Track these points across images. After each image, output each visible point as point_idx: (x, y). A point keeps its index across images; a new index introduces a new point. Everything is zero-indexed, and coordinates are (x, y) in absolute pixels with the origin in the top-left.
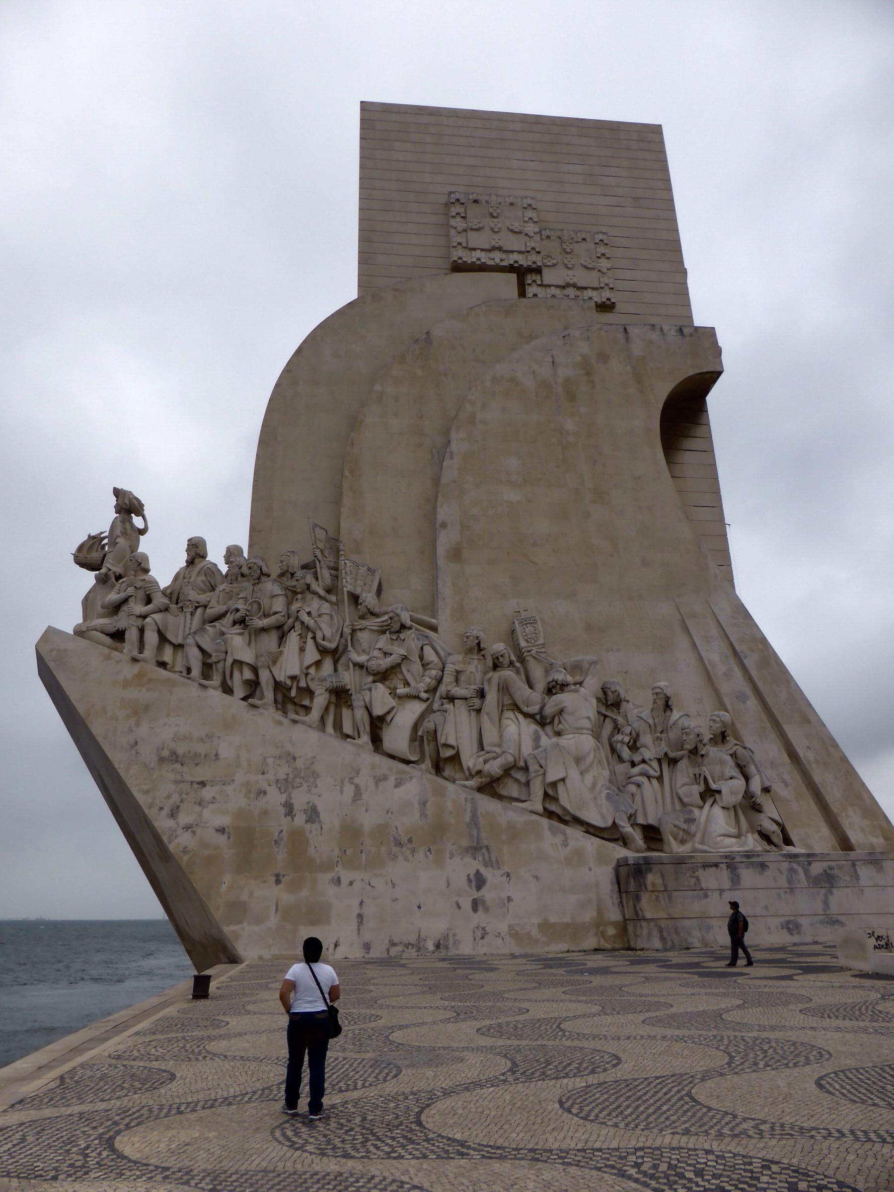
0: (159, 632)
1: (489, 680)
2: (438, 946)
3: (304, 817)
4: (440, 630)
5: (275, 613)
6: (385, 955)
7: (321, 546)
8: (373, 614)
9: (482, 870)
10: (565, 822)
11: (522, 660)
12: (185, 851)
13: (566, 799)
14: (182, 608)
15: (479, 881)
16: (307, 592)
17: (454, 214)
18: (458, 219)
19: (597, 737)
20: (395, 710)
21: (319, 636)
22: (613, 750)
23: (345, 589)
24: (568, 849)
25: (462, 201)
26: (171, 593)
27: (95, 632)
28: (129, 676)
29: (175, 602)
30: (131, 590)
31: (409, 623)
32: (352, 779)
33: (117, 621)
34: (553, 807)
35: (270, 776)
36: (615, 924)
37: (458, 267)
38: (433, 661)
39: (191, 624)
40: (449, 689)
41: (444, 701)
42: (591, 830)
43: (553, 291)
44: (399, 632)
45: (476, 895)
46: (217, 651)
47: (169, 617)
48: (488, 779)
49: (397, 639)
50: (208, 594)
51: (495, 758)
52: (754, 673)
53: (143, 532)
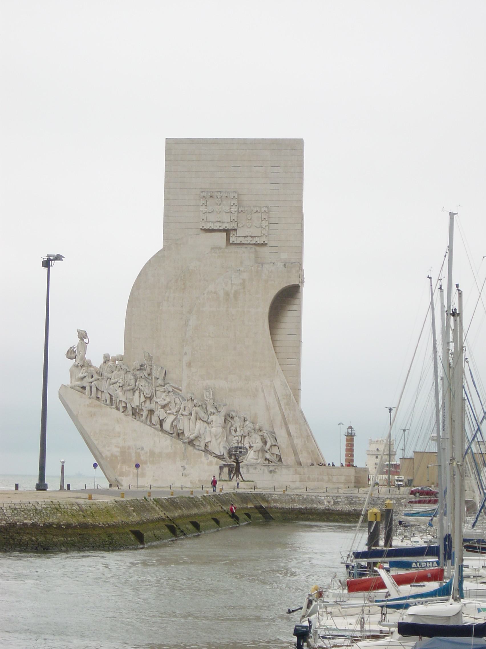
0: (96, 387)
1: (193, 410)
4: (182, 390)
5: (131, 385)
7: (146, 358)
8: (161, 386)
9: (185, 465)
17: (202, 204)
18: (204, 207)
24: (209, 461)
26: (99, 373)
30: (86, 374)
44: (168, 393)
50: (111, 374)
51: (192, 434)
52: (283, 407)
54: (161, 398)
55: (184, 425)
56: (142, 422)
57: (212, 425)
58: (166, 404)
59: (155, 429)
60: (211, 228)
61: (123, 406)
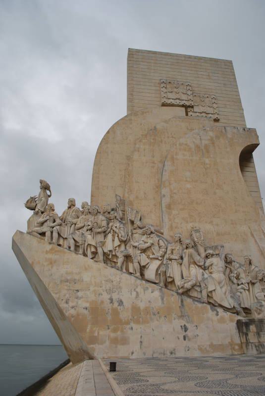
0: (58, 233)
1: (185, 253)
2: (171, 353)
3: (117, 304)
4: (164, 234)
5: (103, 227)
6: (151, 357)
8: (139, 228)
9: (187, 324)
11: (196, 245)
12: (73, 316)
14: (66, 224)
15: (186, 329)
16: (115, 219)
18: (164, 88)
19: (224, 274)
22: (230, 279)
26: (62, 219)
28: (48, 249)
30: (48, 217)
31: (153, 231)
32: (135, 289)
34: (211, 301)
35: (104, 288)
36: (238, 345)
37: (164, 105)
42: (226, 309)
43: (198, 114)
44: (150, 234)
45: (184, 334)
46: (82, 240)
47: (62, 228)
51: (188, 282)
53: (49, 196)
54: (140, 240)
55: (174, 271)
56: (118, 269)
57: (212, 270)
58: (148, 248)
59: (137, 277)
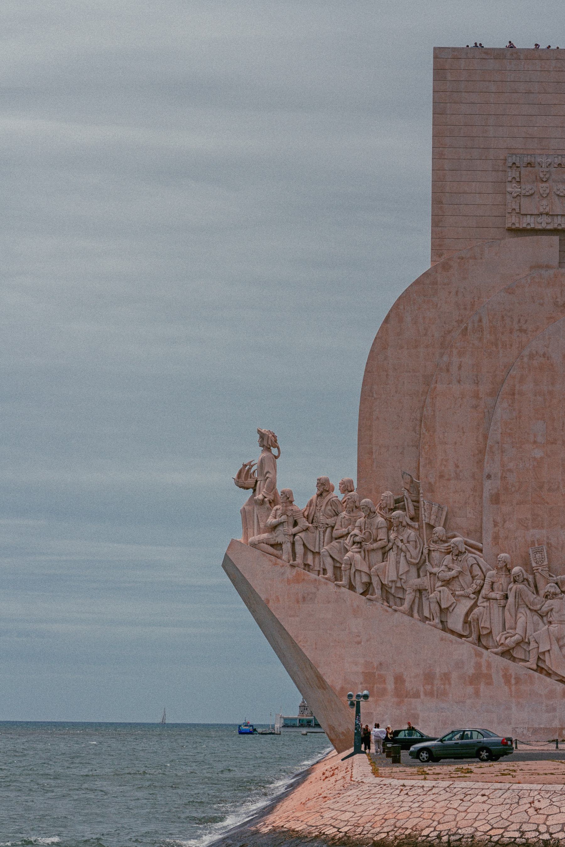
0: (304, 545)
1: (511, 589)
5: (380, 540)
8: (441, 540)
10: (549, 675)
13: (549, 662)
14: (317, 527)
17: (510, 179)
20: (454, 605)
21: (408, 556)
23: (424, 522)
25: (518, 164)
26: (308, 515)
27: (262, 544)
28: (290, 577)
29: (311, 522)
30: (284, 518)
33: (276, 537)
38: (478, 575)
39: (324, 539)
40: (487, 593)
41: (485, 600)
48: (508, 648)
49: (456, 560)
50: (333, 519)
51: (511, 637)
57: (551, 619)
60: (529, 227)
61: (363, 581)
